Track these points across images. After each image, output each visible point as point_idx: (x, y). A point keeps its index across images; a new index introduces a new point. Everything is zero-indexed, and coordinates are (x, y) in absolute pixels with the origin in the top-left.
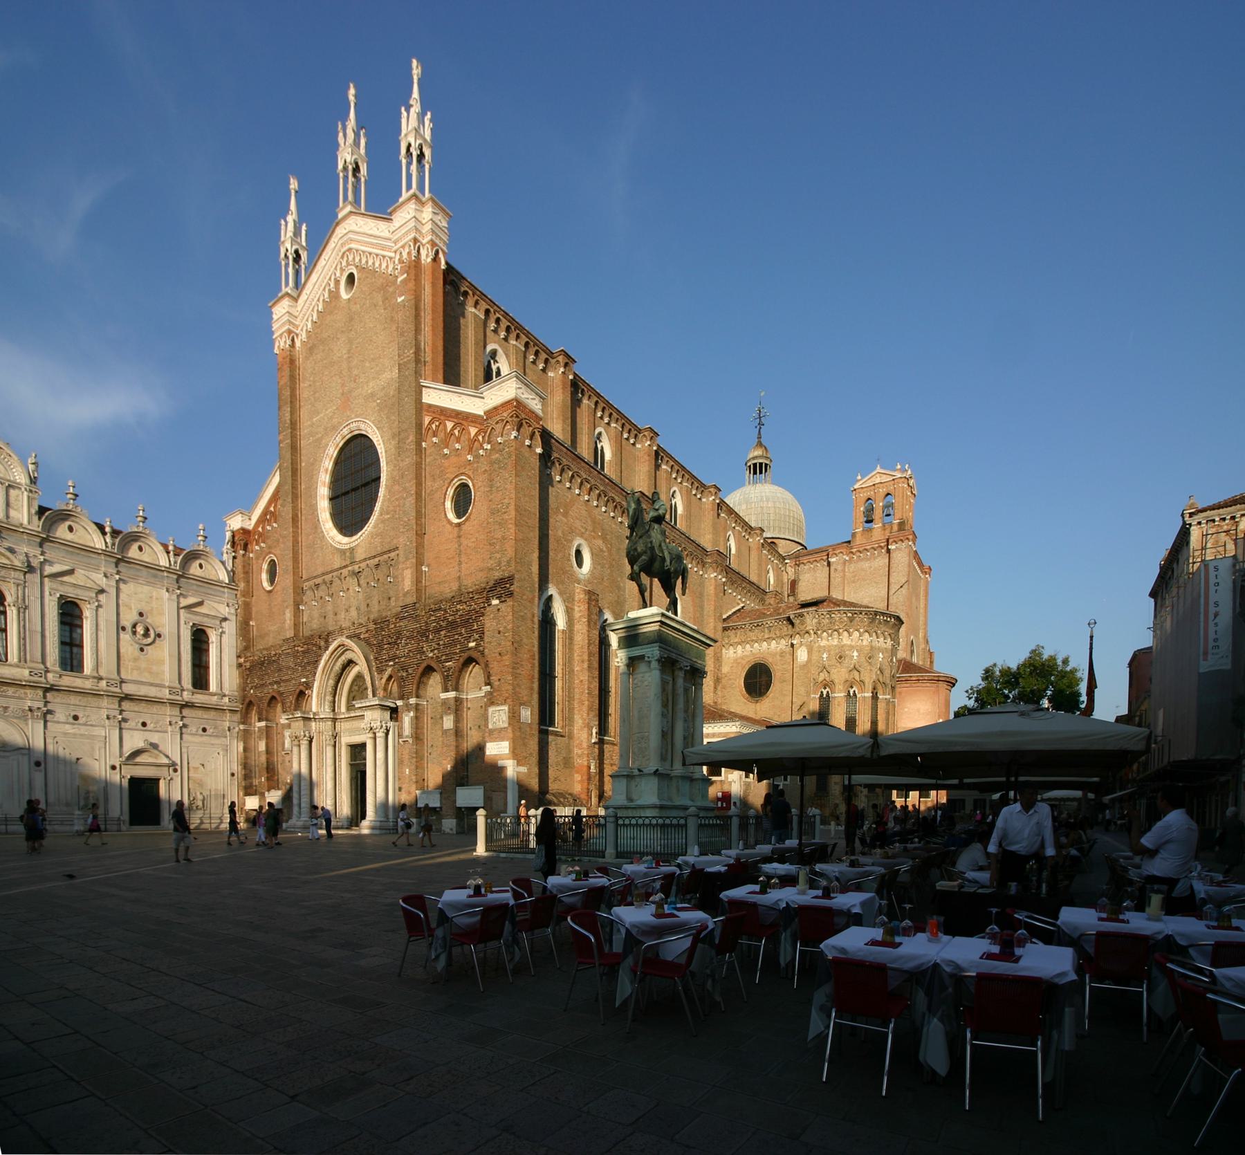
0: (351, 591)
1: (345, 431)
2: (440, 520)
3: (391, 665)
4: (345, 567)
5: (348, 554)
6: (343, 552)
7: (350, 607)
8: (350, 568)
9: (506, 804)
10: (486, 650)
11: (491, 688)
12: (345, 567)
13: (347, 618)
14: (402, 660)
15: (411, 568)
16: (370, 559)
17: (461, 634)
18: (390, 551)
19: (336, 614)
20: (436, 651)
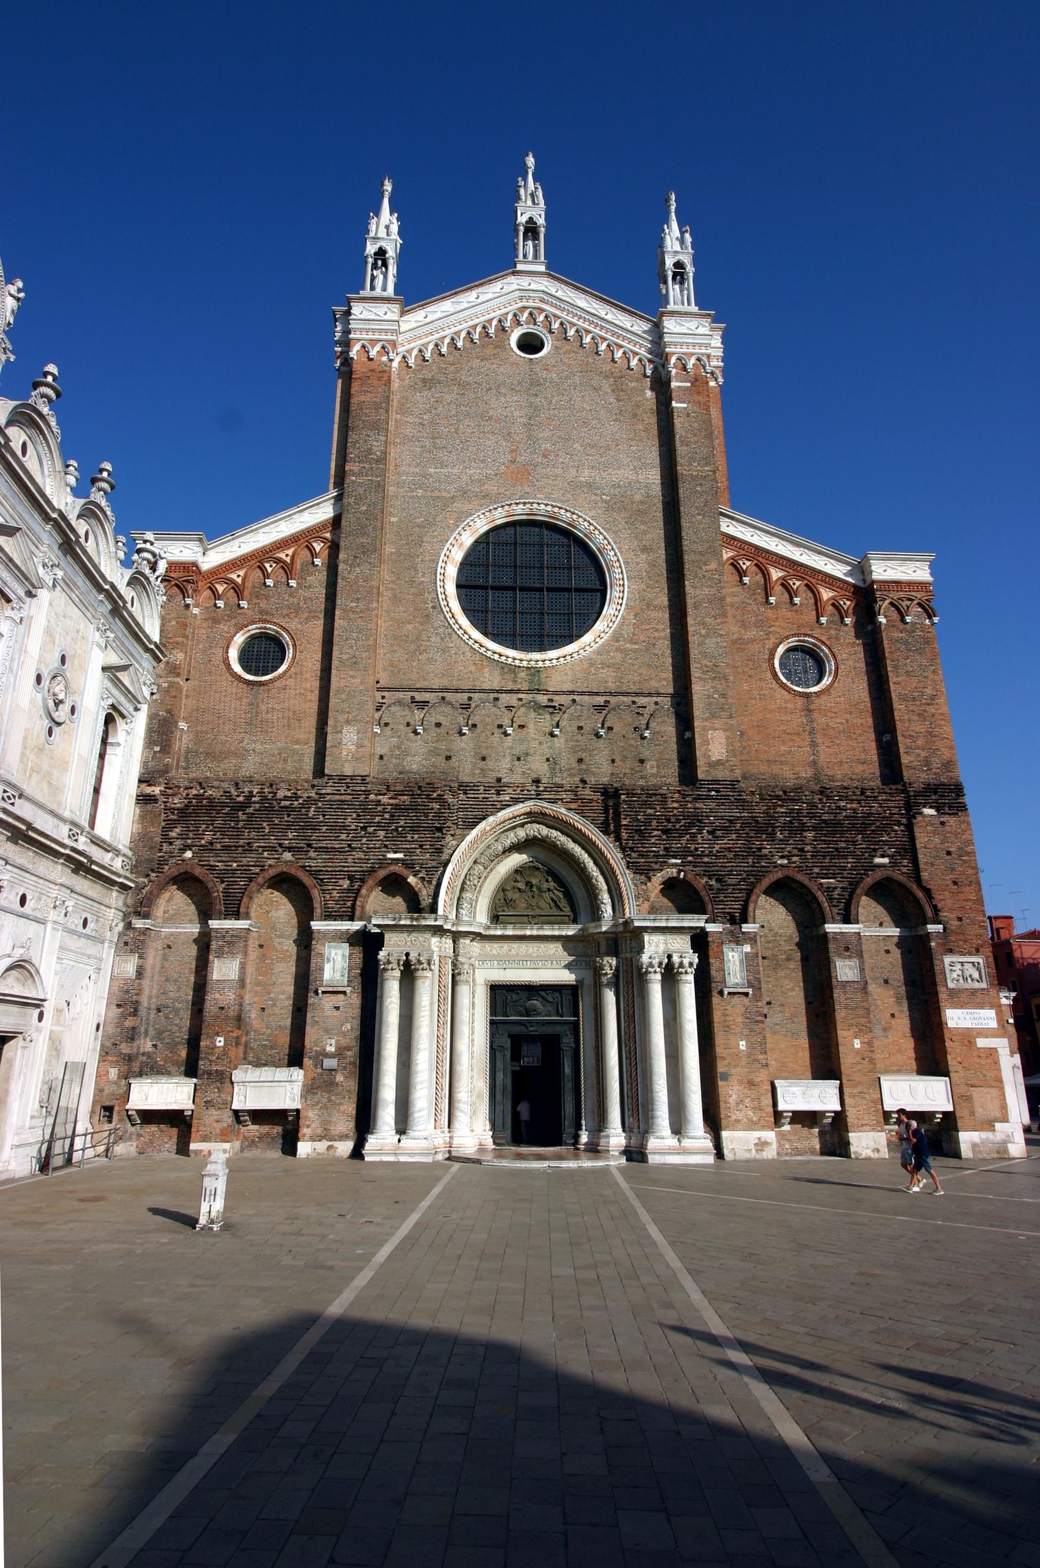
0: (531, 729)
1: (519, 509)
2: (761, 679)
3: (675, 865)
4: (511, 691)
5: (523, 674)
6: (512, 670)
7: (527, 754)
8: (521, 696)
9: (1004, 1107)
10: (925, 875)
11: (945, 929)
12: (511, 691)
13: (519, 770)
14: (706, 859)
15: (725, 730)
16: (582, 693)
17: (854, 843)
18: (637, 694)
19: (484, 759)
20: (794, 859)
